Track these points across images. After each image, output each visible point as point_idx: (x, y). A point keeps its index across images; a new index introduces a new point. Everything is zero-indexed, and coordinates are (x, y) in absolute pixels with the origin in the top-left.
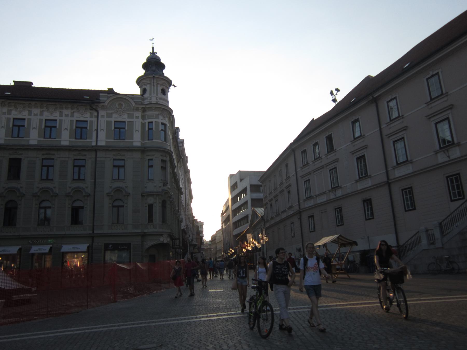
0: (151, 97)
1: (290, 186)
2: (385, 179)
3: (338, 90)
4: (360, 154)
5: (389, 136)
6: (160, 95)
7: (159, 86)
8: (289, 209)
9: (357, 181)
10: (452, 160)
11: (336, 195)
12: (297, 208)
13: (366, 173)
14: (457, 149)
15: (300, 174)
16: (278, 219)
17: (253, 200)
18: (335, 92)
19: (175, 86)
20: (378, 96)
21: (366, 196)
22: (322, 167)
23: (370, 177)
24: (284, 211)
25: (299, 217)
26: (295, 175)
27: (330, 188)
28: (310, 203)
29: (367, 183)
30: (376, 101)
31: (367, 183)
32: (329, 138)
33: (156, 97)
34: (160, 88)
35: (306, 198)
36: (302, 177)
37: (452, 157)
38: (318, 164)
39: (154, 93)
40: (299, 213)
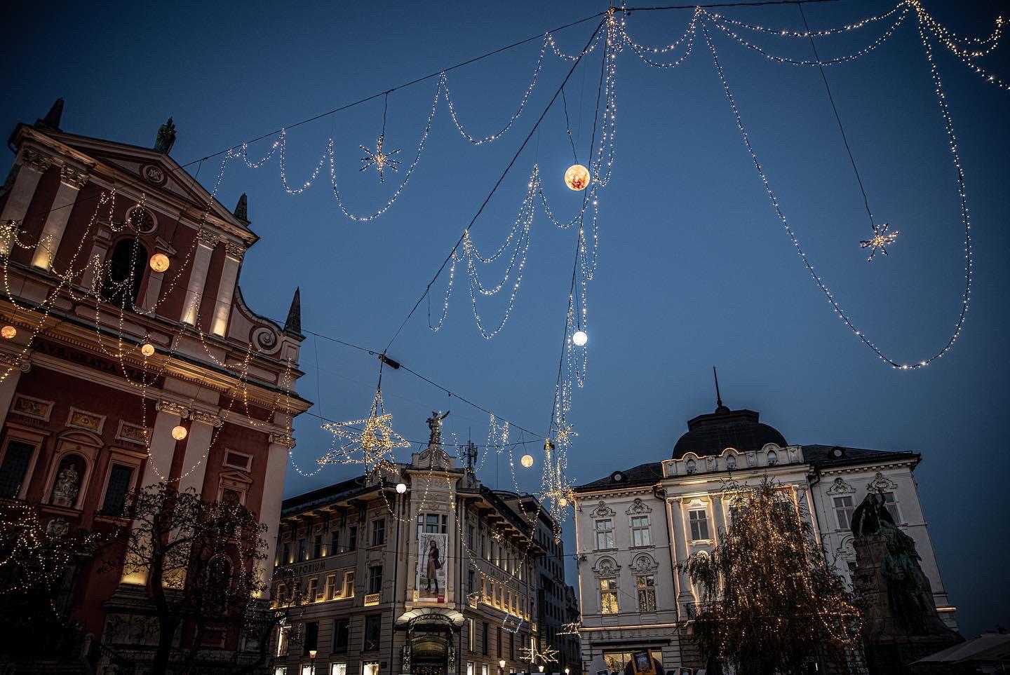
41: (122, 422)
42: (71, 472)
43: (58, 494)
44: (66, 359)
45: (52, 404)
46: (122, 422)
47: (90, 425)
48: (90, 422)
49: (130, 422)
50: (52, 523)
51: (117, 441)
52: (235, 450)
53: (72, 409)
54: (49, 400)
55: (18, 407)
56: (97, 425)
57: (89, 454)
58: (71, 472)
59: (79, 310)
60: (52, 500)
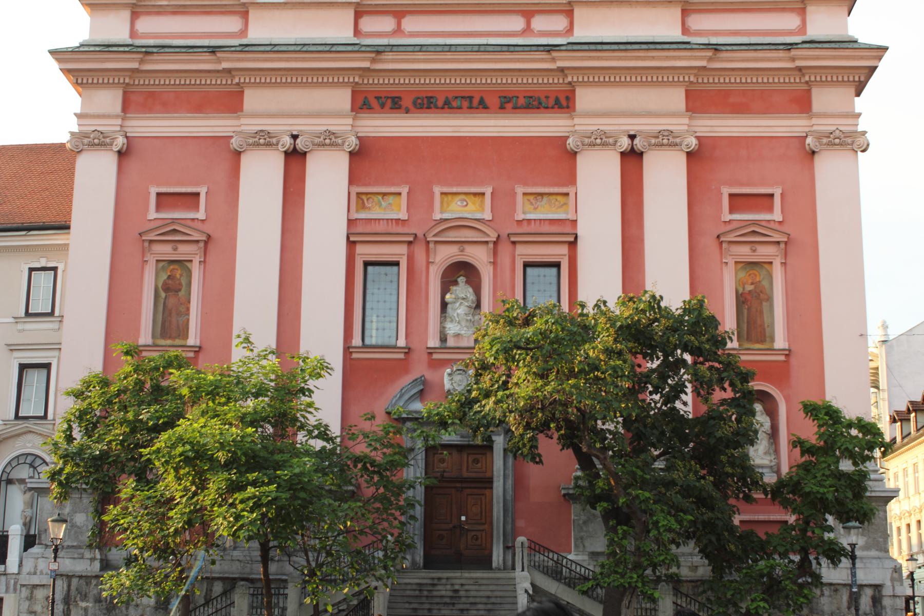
41: (520, 190)
42: (462, 290)
43: (452, 328)
44: (407, 111)
45: (404, 190)
46: (520, 190)
47: (471, 207)
48: (470, 204)
49: (535, 184)
50: (450, 375)
51: (519, 222)
52: (742, 185)
53: (437, 190)
54: (398, 185)
55: (362, 206)
56: (482, 206)
57: (479, 257)
58: (462, 290)
59: (410, 24)
60: (443, 339)
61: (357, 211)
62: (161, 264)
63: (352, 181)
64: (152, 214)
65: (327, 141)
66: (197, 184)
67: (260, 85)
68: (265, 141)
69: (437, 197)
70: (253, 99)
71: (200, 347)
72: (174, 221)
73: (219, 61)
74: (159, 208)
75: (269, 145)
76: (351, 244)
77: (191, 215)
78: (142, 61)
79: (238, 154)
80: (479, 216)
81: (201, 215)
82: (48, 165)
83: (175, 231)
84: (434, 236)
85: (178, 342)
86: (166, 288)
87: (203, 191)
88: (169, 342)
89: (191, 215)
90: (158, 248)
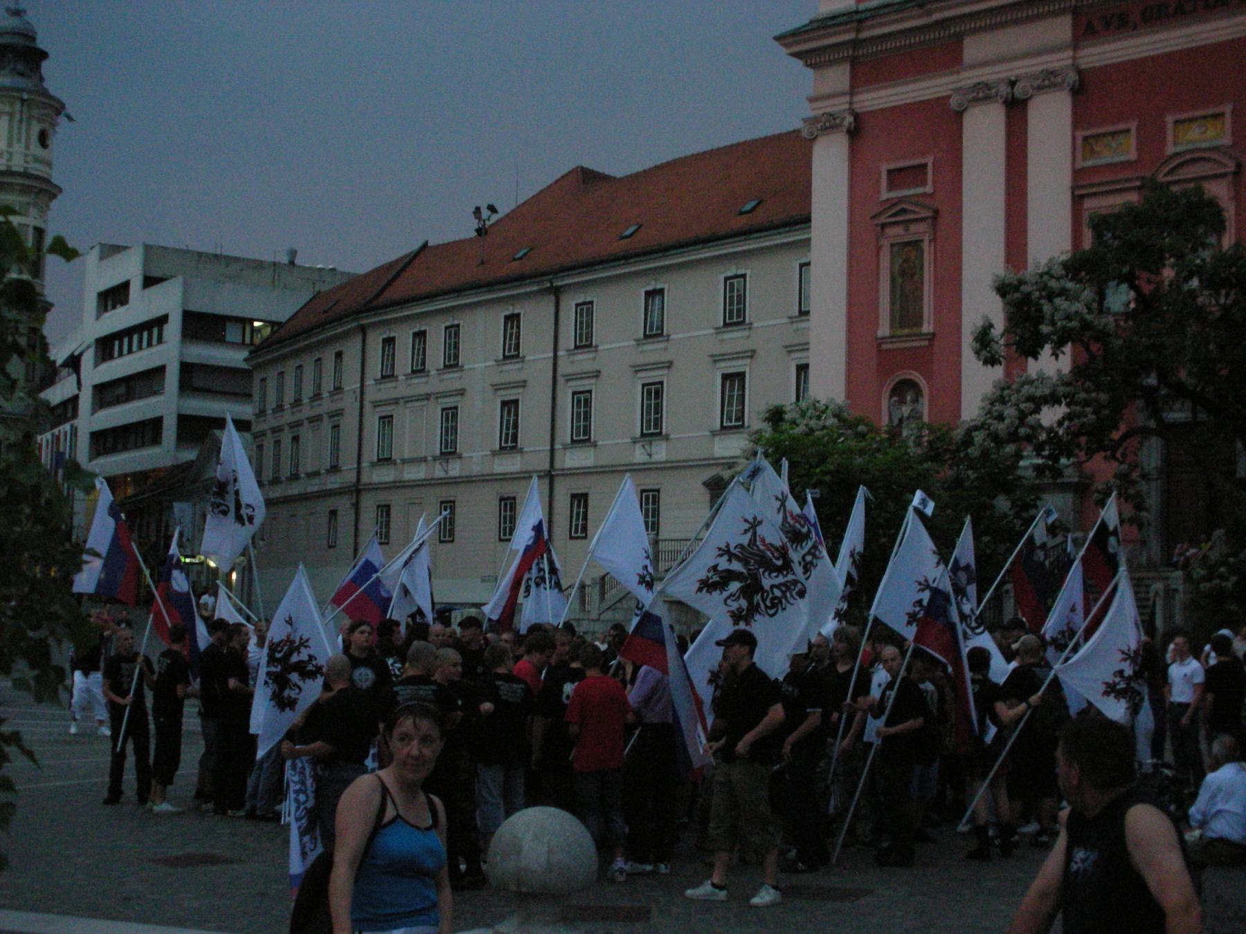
0: (11, 154)
1: (339, 413)
2: (546, 466)
3: (492, 209)
4: (510, 395)
5: (570, 378)
6: (36, 148)
7: (34, 122)
8: (328, 471)
9: (494, 453)
10: (656, 463)
11: (446, 472)
12: (352, 477)
13: (515, 438)
14: (664, 444)
15: (371, 395)
16: (294, 489)
17: (187, 369)
18: (485, 213)
19: (70, 118)
20: (562, 286)
21: (508, 489)
22: (427, 397)
23: (521, 451)
24: (316, 474)
25: (354, 501)
26: (358, 391)
27: (438, 453)
28: (385, 475)
29: (511, 464)
30: (557, 292)
31: (511, 464)
32: (453, 332)
33: (26, 155)
34: (36, 129)
35: (379, 460)
36: (376, 404)
37: (656, 458)
38: (419, 386)
39: (19, 140)
40: (356, 490)
45: (1133, 125)
53: (1170, 119)
55: (1093, 153)
61: (1084, 159)
62: (896, 249)
63: (1077, 124)
64: (885, 195)
65: (1047, 82)
66: (923, 154)
67: (975, 31)
68: (982, 93)
69: (1170, 126)
70: (974, 48)
71: (934, 334)
72: (900, 200)
73: (929, 14)
74: (891, 187)
75: (987, 98)
76: (1077, 200)
77: (920, 190)
78: (858, 31)
79: (959, 114)
80: (1218, 143)
81: (929, 189)
82: (785, 157)
83: (904, 211)
84: (1165, 175)
85: (915, 330)
86: (903, 273)
87: (929, 160)
88: (906, 331)
89: (920, 190)
90: (890, 231)
